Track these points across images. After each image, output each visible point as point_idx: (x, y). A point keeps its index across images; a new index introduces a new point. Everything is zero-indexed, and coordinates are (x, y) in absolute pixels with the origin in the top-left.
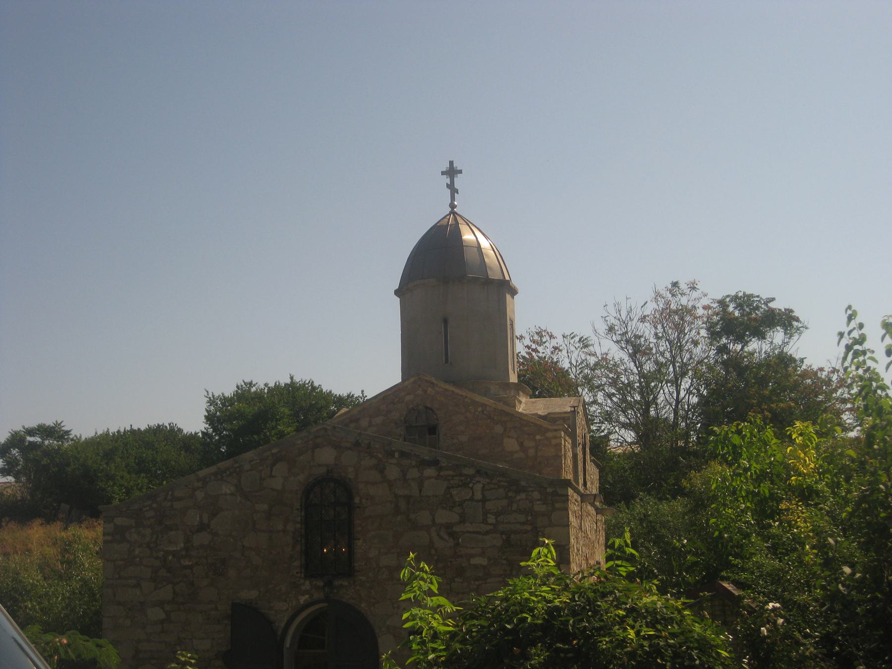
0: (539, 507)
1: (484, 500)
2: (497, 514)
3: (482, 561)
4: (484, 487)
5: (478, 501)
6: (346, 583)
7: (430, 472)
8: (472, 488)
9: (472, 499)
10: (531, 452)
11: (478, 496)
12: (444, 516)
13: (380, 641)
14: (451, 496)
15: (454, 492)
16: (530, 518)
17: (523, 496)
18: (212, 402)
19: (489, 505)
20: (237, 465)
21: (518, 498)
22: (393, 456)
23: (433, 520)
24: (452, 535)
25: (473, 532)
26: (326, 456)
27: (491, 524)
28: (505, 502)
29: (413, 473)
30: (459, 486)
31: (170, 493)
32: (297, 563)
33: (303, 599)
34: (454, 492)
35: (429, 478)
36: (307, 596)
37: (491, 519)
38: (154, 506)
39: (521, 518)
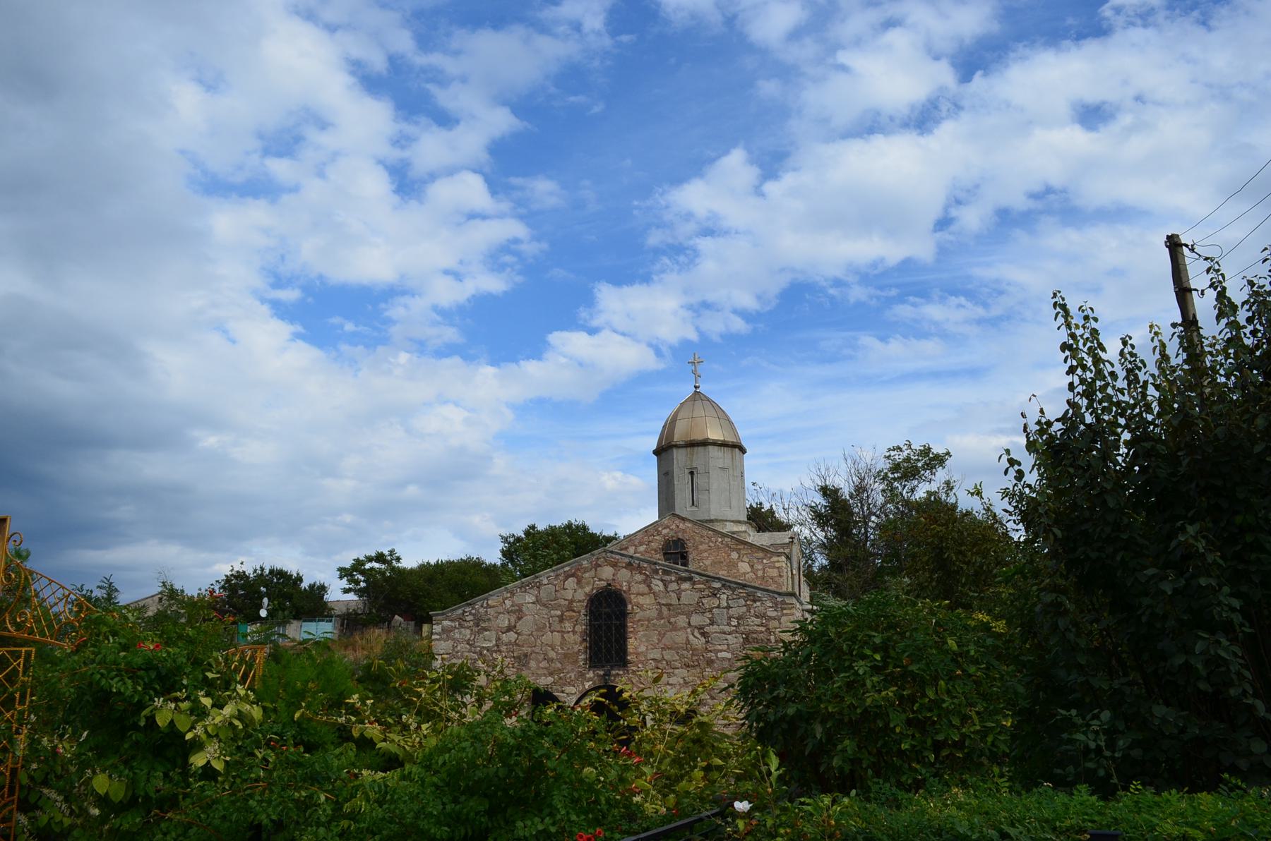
0: (771, 613)
1: (729, 607)
3: (729, 655)
7: (686, 586)
9: (718, 607)
10: (760, 573)
12: (696, 620)
15: (705, 601)
17: (758, 604)
18: (505, 539)
26: (607, 572)
28: (745, 609)
29: (674, 586)
33: (588, 685)
34: (705, 601)
35: (685, 590)
37: (734, 622)
39: (758, 621)
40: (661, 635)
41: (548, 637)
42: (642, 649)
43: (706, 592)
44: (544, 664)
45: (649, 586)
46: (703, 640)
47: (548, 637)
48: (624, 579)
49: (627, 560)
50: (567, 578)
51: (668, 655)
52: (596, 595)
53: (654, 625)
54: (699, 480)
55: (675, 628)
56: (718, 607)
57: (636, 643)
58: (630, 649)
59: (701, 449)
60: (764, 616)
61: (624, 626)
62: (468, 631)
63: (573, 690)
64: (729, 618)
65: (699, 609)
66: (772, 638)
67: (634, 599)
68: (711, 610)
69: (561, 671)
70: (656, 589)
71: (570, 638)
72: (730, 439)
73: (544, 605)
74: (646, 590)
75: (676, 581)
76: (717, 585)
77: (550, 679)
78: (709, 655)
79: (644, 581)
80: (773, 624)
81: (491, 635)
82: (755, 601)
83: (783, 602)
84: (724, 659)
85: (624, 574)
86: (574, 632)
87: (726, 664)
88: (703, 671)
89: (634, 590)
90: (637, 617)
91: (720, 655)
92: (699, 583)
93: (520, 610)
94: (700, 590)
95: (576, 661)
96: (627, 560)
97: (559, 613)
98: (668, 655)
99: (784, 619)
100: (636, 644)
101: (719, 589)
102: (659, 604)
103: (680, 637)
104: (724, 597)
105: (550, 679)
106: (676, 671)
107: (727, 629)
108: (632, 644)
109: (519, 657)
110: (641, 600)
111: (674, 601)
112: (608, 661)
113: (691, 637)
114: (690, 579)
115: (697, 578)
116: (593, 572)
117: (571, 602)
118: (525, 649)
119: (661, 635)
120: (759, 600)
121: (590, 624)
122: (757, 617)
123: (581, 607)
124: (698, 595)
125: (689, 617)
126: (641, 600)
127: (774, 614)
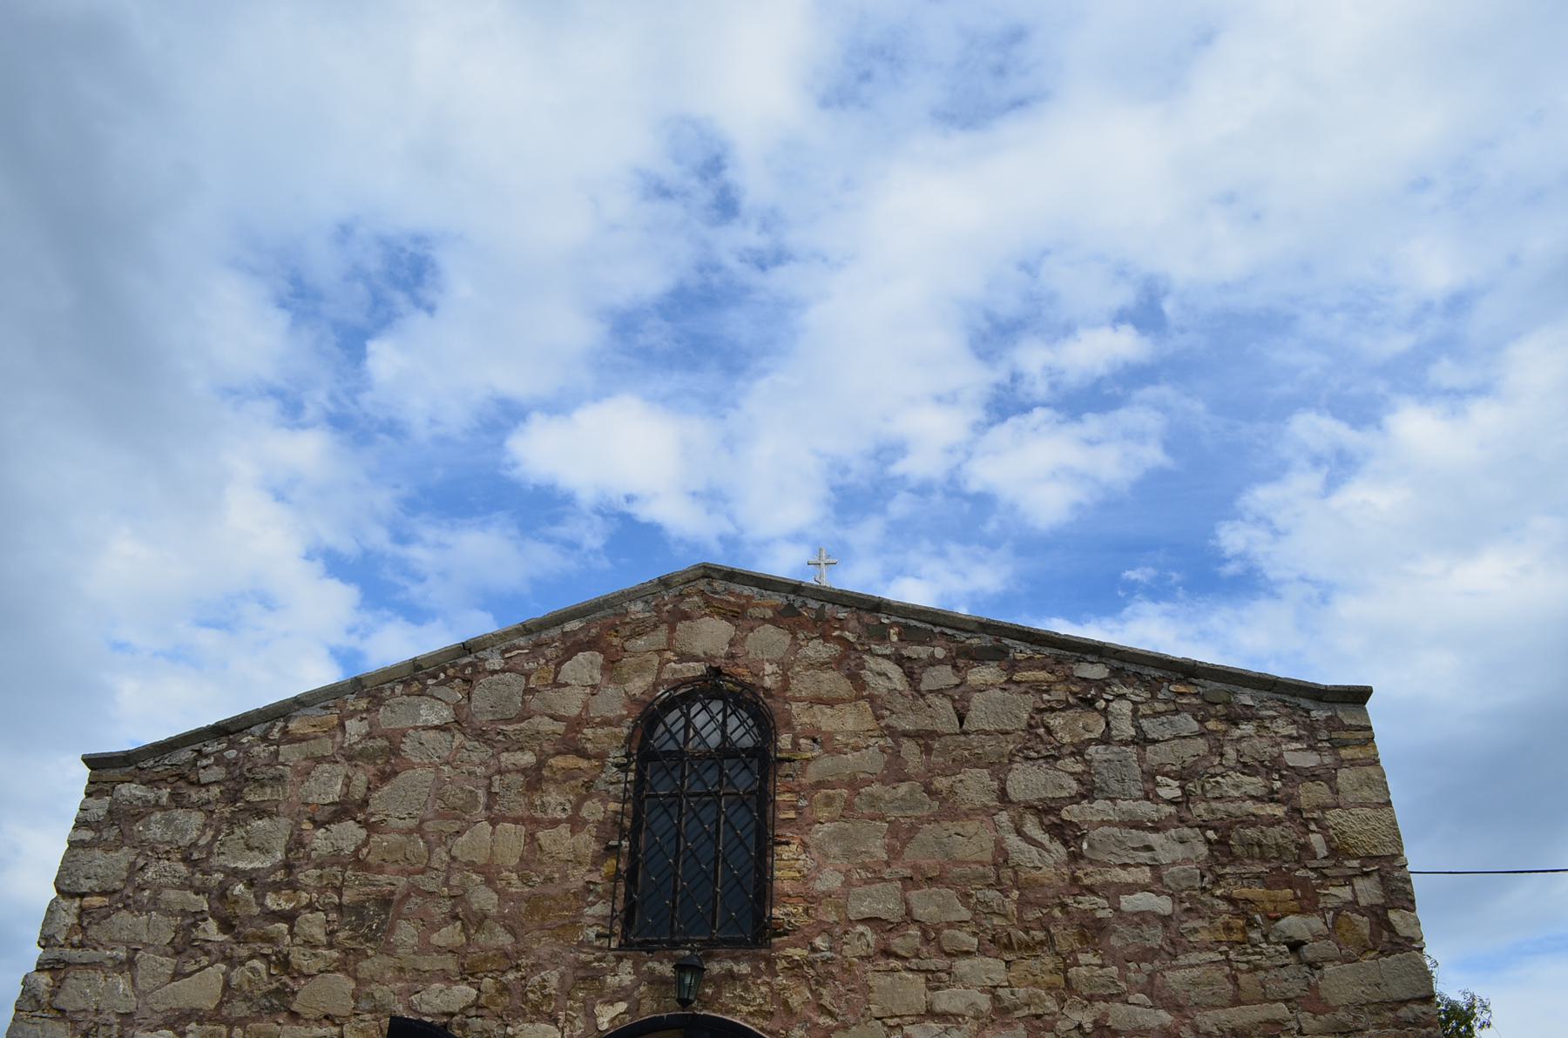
0: (1298, 757)
1: (1142, 740)
2: (1182, 776)
3: (1164, 905)
4: (1135, 711)
5: (1125, 743)
6: (744, 968)
8: (1105, 712)
11: (1126, 729)
12: (1027, 781)
14: (1049, 731)
15: (1055, 721)
16: (1278, 784)
17: (1248, 728)
19: (1154, 755)
21: (1237, 733)
22: (883, 638)
23: (1003, 795)
24: (1062, 831)
27: (1171, 802)
28: (1201, 745)
29: (943, 676)
30: (1069, 706)
31: (280, 724)
32: (601, 909)
34: (1055, 721)
36: (622, 1007)
37: (1170, 790)
38: (232, 754)
39: (1254, 784)
40: (901, 835)
41: (477, 841)
42: (830, 881)
43: (1059, 693)
44: (450, 935)
45: (855, 678)
47: (477, 841)
48: (766, 653)
49: (778, 599)
50: (568, 654)
51: (927, 903)
53: (874, 800)
55: (950, 809)
56: (1105, 740)
58: (784, 877)
60: (1274, 766)
61: (762, 800)
62: (198, 818)
64: (1150, 776)
65: (1037, 743)
66: (1316, 840)
67: (801, 715)
69: (509, 959)
70: (879, 686)
71: (558, 841)
73: (480, 735)
74: (845, 688)
75: (952, 661)
76: (1097, 671)
77: (463, 993)
78: (1087, 902)
80: (1310, 794)
81: (273, 831)
82: (1234, 721)
83: (1333, 723)
84: (1143, 917)
86: (576, 823)
87: (1156, 937)
88: (1067, 962)
89: (803, 685)
90: (812, 774)
91: (1128, 903)
92: (1030, 663)
93: (394, 750)
94: (1036, 688)
95: (575, 924)
96: (778, 599)
97: (528, 758)
98: (927, 903)
99: (1345, 777)
100: (813, 863)
101: (1102, 685)
102: (891, 732)
103: (972, 843)
104: (1125, 707)
105: (463, 993)
106: (962, 965)
107: (1146, 809)
109: (358, 909)
110: (826, 720)
111: (944, 719)
113: (1013, 841)
114: (997, 654)
115: (1021, 651)
116: (662, 634)
117: (576, 724)
118: (390, 880)
119: (901, 835)
120: (1249, 715)
121: (639, 794)
122: (1246, 768)
123: (610, 741)
124: (1031, 700)
125: (999, 768)
126: (826, 720)
127: (1310, 760)
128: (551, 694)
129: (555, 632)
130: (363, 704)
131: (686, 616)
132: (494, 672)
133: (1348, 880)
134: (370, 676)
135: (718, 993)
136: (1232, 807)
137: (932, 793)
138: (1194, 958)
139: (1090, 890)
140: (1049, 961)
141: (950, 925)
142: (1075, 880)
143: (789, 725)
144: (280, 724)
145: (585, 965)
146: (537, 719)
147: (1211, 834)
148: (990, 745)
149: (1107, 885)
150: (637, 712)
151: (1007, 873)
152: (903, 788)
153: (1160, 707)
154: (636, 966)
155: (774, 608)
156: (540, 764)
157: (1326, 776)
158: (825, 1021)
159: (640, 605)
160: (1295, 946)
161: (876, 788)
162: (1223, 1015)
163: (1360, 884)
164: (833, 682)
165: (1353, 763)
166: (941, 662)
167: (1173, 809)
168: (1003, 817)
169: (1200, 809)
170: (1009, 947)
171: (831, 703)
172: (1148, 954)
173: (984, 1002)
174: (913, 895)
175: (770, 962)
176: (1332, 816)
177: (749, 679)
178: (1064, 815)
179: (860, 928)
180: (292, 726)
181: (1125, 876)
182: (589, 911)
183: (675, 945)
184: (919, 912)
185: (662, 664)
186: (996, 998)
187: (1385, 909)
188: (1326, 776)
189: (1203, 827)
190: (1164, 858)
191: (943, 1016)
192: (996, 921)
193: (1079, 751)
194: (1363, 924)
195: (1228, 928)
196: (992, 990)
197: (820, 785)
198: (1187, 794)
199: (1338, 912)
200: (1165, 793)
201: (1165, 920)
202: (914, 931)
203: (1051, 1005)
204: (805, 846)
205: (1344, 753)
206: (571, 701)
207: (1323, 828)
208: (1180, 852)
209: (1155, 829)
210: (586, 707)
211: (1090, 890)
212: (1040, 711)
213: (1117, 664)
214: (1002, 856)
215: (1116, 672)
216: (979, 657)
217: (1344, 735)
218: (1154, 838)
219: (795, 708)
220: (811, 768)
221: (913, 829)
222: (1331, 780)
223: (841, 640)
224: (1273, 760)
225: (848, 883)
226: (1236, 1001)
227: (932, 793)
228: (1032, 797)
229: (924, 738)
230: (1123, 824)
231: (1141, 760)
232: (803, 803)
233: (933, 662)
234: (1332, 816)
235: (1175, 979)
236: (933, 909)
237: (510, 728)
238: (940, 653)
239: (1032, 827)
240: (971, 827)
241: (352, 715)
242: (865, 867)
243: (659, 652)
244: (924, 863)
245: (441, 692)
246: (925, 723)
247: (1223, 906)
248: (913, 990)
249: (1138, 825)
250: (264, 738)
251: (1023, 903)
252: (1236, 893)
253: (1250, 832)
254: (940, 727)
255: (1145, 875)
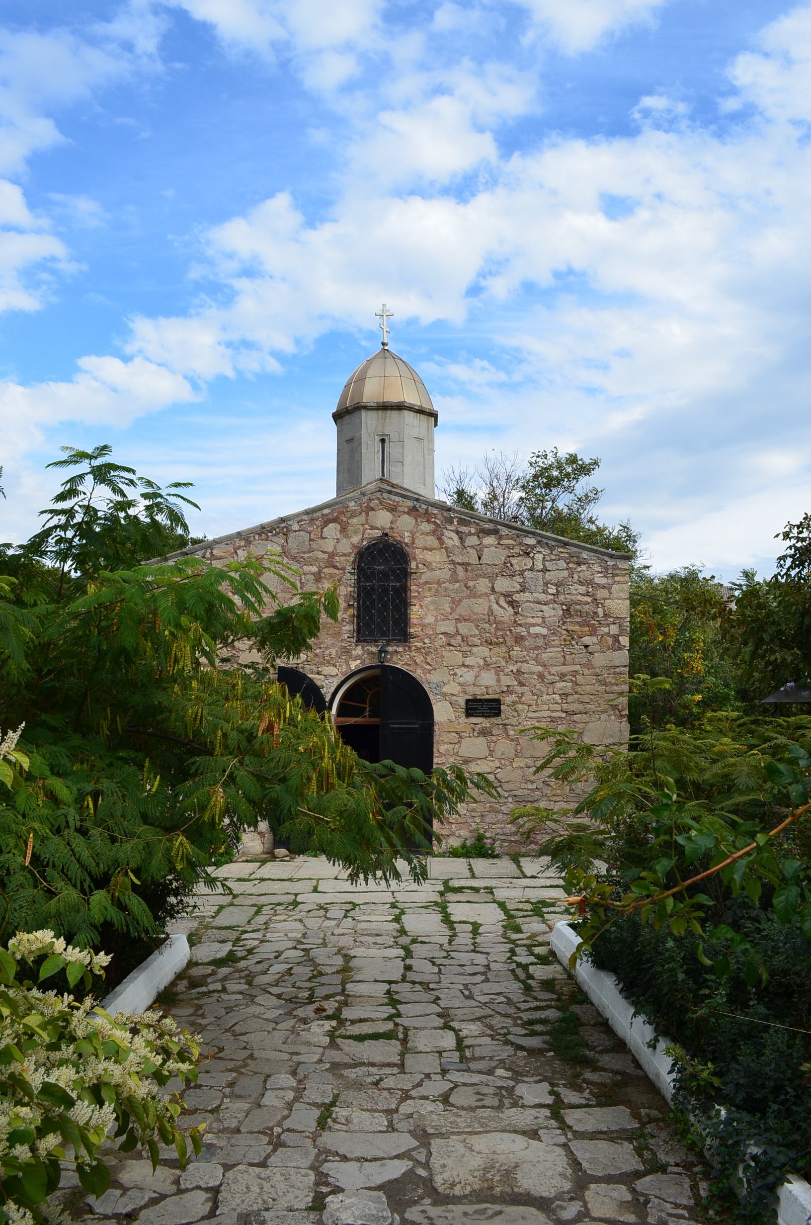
0: (600, 580)
1: (545, 570)
3: (544, 631)
4: (544, 558)
7: (490, 540)
9: (532, 569)
12: (502, 584)
13: (434, 707)
14: (512, 565)
15: (514, 561)
17: (584, 567)
19: (548, 576)
20: (283, 525)
21: (579, 569)
22: (451, 523)
23: (493, 589)
24: (512, 603)
25: (534, 602)
26: (383, 519)
28: (566, 573)
29: (473, 540)
30: (520, 555)
31: (209, 551)
32: (348, 627)
33: (354, 665)
34: (514, 561)
36: (359, 662)
37: (552, 590)
39: (582, 590)
40: (456, 603)
42: (430, 619)
43: (517, 550)
45: (439, 539)
46: (511, 610)
48: (405, 528)
49: (410, 503)
50: (326, 523)
51: (464, 628)
52: (368, 548)
53: (446, 589)
54: (392, 449)
55: (473, 594)
56: (532, 569)
57: (421, 612)
59: (395, 413)
60: (590, 583)
61: (405, 589)
63: (332, 670)
64: (546, 584)
65: (506, 570)
67: (420, 554)
68: (521, 574)
70: (449, 543)
72: (426, 406)
73: (294, 559)
74: (436, 543)
76: (531, 541)
78: (519, 629)
79: (434, 532)
80: (601, 594)
82: (579, 564)
83: (615, 567)
84: (537, 635)
85: (406, 523)
87: (540, 642)
88: (510, 649)
89: (420, 542)
90: (424, 579)
91: (533, 630)
92: (508, 537)
94: (508, 547)
95: (339, 633)
96: (410, 503)
97: (314, 569)
98: (464, 628)
100: (423, 612)
101: (533, 547)
102: (453, 562)
103: (480, 607)
104: (540, 556)
106: (475, 649)
108: (415, 613)
110: (429, 556)
111: (474, 559)
112: (384, 634)
113: (495, 606)
114: (495, 532)
115: (504, 531)
117: (332, 555)
119: (456, 603)
120: (584, 562)
122: (581, 583)
123: (347, 563)
124: (506, 552)
125: (492, 578)
126: (429, 556)
127: (603, 581)
128: (320, 541)
129: (319, 514)
130: (243, 543)
131: (373, 509)
132: (296, 531)
133: (608, 625)
134: (243, 531)
135: (392, 657)
136: (573, 598)
137: (467, 587)
138: (552, 649)
139: (520, 625)
140: (504, 649)
141: (471, 636)
142: (515, 621)
143: (415, 559)
144: (209, 551)
145: (345, 647)
146: (316, 552)
147: (564, 607)
148: (490, 570)
149: (526, 624)
150: (356, 551)
151: (492, 618)
152: (457, 585)
153: (553, 557)
154: (362, 647)
155: (408, 507)
156: (320, 572)
157: (608, 587)
158: (428, 667)
159: (353, 503)
160: (586, 647)
161: (447, 584)
162: (559, 668)
163: (612, 627)
164: (432, 541)
165: (619, 582)
166: (473, 534)
167: (552, 597)
168: (492, 597)
169: (562, 597)
170: (491, 644)
171: (431, 550)
172: (537, 648)
173: (482, 662)
174: (459, 625)
175: (409, 647)
176: (607, 602)
177: (399, 539)
178: (514, 598)
179: (441, 636)
180: (215, 552)
181: (532, 621)
182: (344, 628)
183: (376, 641)
184: (461, 631)
185: (364, 531)
186: (485, 661)
187: (618, 636)
188: (608, 587)
189: (562, 604)
190: (547, 615)
191: (468, 666)
192: (487, 635)
193: (521, 574)
194: (610, 641)
195: (565, 640)
196: (484, 658)
197: (426, 583)
198: (558, 591)
199: (602, 636)
200: (550, 591)
201: (544, 637)
202: (459, 638)
203: (503, 664)
204: (421, 606)
205: (617, 579)
206: (329, 546)
207: (603, 606)
208: (553, 613)
209: (545, 605)
210: (335, 548)
211: (520, 625)
212: (509, 557)
213: (540, 539)
214: (491, 611)
215: (539, 542)
216: (488, 533)
217: (618, 572)
218: (544, 608)
219: (417, 551)
220: (423, 576)
221: (460, 601)
222: (609, 589)
223: (435, 523)
224: (591, 580)
225: (436, 620)
226: (564, 664)
227: (467, 587)
228: (503, 591)
229: (465, 565)
230: (534, 602)
231: (544, 578)
232: (420, 590)
233: (470, 534)
234: (607, 602)
235: (545, 656)
236: (466, 630)
237: (305, 556)
238: (473, 530)
239: (502, 602)
240: (481, 601)
241: (239, 548)
242: (442, 614)
243: (363, 525)
244: (464, 613)
245: (275, 539)
246: (466, 560)
247: (565, 632)
248: (458, 657)
249: (539, 603)
250: (204, 557)
251: (497, 629)
252: (569, 628)
253: (578, 607)
254: (471, 562)
255: (539, 621)
